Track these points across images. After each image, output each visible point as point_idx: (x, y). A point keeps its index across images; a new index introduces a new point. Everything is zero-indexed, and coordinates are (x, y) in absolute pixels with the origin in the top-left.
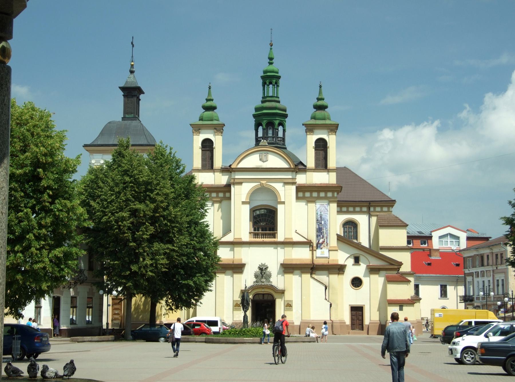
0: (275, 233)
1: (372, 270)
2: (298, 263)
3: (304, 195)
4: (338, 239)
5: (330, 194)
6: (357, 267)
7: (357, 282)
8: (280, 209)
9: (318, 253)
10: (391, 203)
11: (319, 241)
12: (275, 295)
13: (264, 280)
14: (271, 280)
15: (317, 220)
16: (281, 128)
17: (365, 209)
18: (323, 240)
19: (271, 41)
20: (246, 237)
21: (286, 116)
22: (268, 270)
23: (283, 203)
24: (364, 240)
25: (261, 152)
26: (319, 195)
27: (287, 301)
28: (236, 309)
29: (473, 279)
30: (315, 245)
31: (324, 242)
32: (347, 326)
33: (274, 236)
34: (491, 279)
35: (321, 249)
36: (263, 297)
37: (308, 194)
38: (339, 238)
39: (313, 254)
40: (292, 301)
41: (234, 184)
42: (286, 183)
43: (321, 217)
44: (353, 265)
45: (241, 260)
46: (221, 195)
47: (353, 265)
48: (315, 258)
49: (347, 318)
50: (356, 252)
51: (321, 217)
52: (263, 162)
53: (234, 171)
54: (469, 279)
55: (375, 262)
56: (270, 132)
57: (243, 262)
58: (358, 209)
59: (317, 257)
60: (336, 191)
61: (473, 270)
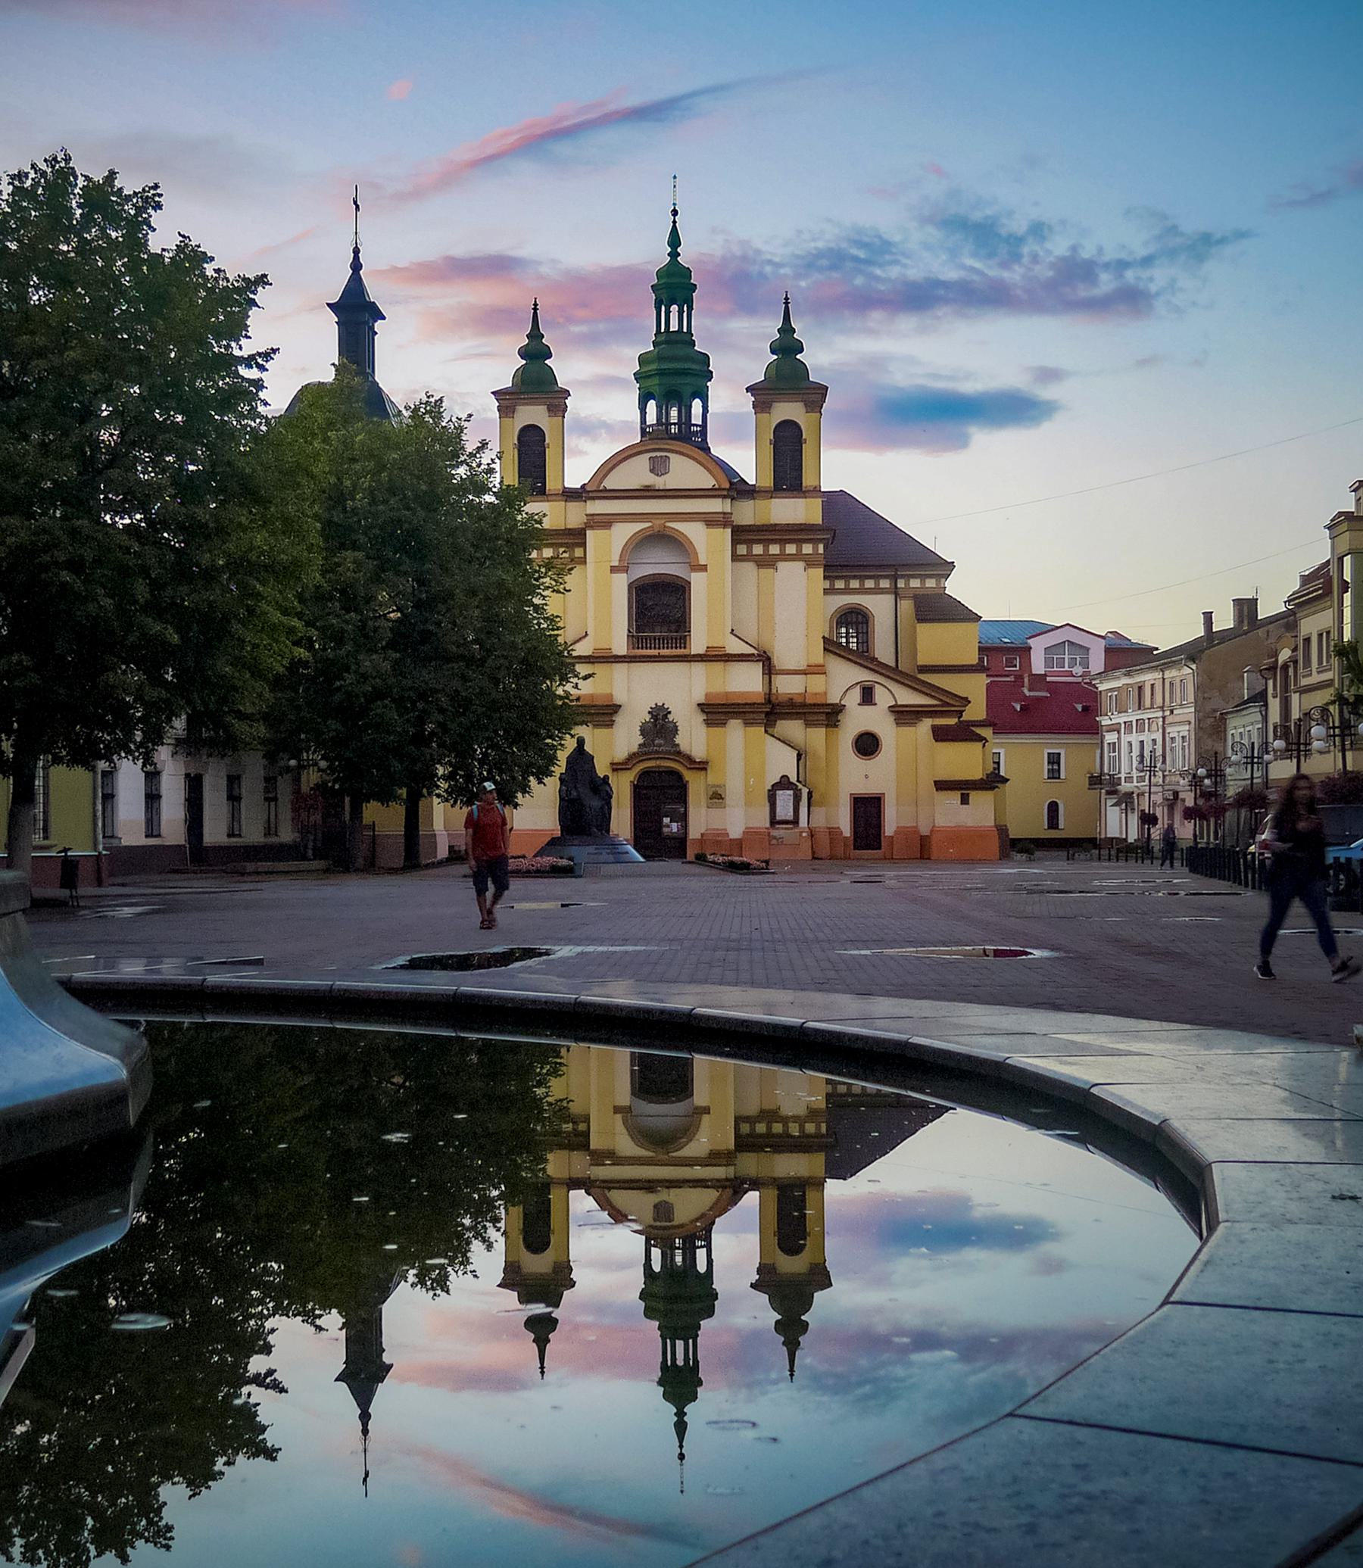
1: (904, 715)
5: (807, 549)
7: (867, 745)
8: (698, 583)
12: (688, 776)
14: (678, 740)
16: (697, 404)
17: (885, 584)
20: (621, 647)
21: (709, 376)
22: (670, 717)
23: (704, 568)
24: (883, 649)
25: (654, 454)
26: (783, 549)
29: (1119, 739)
33: (683, 641)
34: (1158, 736)
37: (758, 549)
41: (592, 528)
42: (711, 521)
48: (774, 691)
50: (865, 676)
53: (593, 498)
54: (1110, 738)
55: (908, 697)
56: (674, 413)
57: (618, 699)
58: (869, 584)
60: (820, 540)
61: (1121, 719)
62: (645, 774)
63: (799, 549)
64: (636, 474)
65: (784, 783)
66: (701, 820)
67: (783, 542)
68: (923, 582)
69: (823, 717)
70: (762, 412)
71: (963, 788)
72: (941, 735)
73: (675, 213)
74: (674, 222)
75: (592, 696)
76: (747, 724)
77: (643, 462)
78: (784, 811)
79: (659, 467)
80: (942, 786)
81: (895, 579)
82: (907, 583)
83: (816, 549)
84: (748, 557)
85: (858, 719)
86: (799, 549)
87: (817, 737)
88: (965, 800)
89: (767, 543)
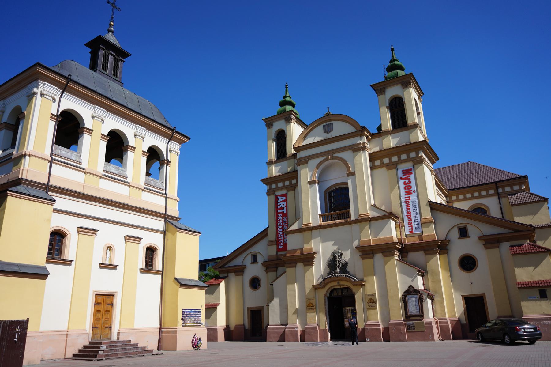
1: (490, 242)
5: (413, 155)
7: (468, 263)
17: (492, 192)
22: (343, 257)
25: (325, 124)
26: (399, 158)
27: (369, 295)
28: (309, 309)
36: (342, 292)
37: (386, 161)
40: (374, 295)
44: (459, 238)
46: (294, 182)
47: (459, 238)
59: (406, 236)
63: (408, 156)
65: (411, 291)
68: (512, 188)
70: (381, 94)
77: (320, 128)
78: (413, 309)
79: (328, 129)
82: (503, 190)
83: (418, 154)
84: (382, 165)
85: (460, 248)
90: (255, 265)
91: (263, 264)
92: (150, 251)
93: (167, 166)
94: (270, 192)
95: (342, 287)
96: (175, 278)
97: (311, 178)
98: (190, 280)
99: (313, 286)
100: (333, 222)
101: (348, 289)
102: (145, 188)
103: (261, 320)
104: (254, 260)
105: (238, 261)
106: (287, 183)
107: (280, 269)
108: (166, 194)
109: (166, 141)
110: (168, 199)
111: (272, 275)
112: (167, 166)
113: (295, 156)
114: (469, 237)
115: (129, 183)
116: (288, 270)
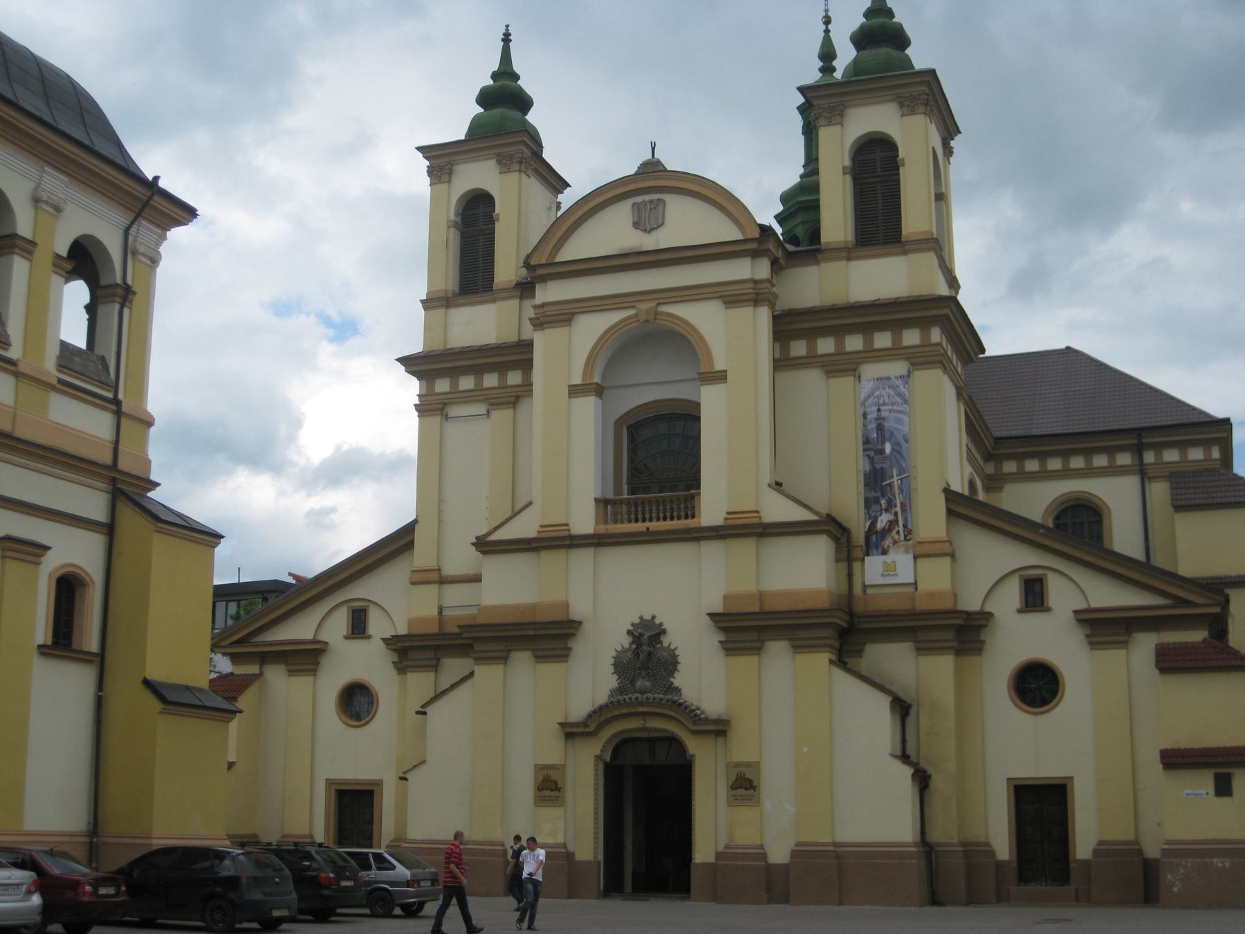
0: (693, 497)
1: (1103, 628)
2: (781, 606)
3: (812, 347)
4: (950, 513)
5: (911, 337)
6: (1035, 620)
7: (1037, 685)
8: (714, 406)
9: (873, 569)
10: (1217, 431)
11: (873, 524)
12: (693, 746)
13: (648, 684)
14: (678, 680)
15: (866, 441)
17: (1124, 459)
18: (892, 517)
19: (826, 11)
20: (584, 521)
22: (666, 640)
23: (721, 377)
25: (639, 199)
26: (868, 342)
27: (737, 765)
30: (859, 537)
31: (893, 524)
32: (1000, 865)
33: (689, 507)
35: (884, 552)
37: (826, 346)
38: (959, 507)
39: (850, 575)
40: (755, 766)
42: (731, 295)
43: (880, 428)
44: (1020, 611)
45: (566, 605)
46: (514, 378)
47: (1020, 611)
48: (858, 590)
49: (998, 832)
51: (880, 428)
52: (645, 231)
53: (544, 279)
55: (1108, 595)
58: (1100, 461)
62: (622, 745)
63: (897, 339)
64: (613, 233)
66: (714, 827)
67: (867, 329)
69: (950, 635)
70: (830, 124)
71: (1221, 765)
72: (1171, 662)
73: (827, 21)
74: (827, 31)
75: (534, 607)
76: (797, 648)
80: (1175, 760)
81: (1138, 450)
83: (926, 336)
84: (811, 361)
85: (1019, 638)
86: (897, 339)
87: (934, 674)
88: (1223, 788)
89: (839, 332)
90: (358, 645)
91: (394, 643)
92: (68, 588)
93: (122, 306)
94: (427, 407)
95: (652, 735)
96: (147, 683)
97: (584, 377)
98: (188, 688)
99: (563, 725)
100: (640, 526)
101: (673, 741)
102: (60, 381)
103: (371, 822)
104: (358, 626)
105: (300, 629)
106: (491, 380)
107: (453, 667)
108: (117, 403)
109: (122, 219)
110: (124, 420)
111: (420, 683)
112: (122, 306)
113: (525, 289)
114: (1049, 610)
115: (12, 363)
116: (480, 671)
